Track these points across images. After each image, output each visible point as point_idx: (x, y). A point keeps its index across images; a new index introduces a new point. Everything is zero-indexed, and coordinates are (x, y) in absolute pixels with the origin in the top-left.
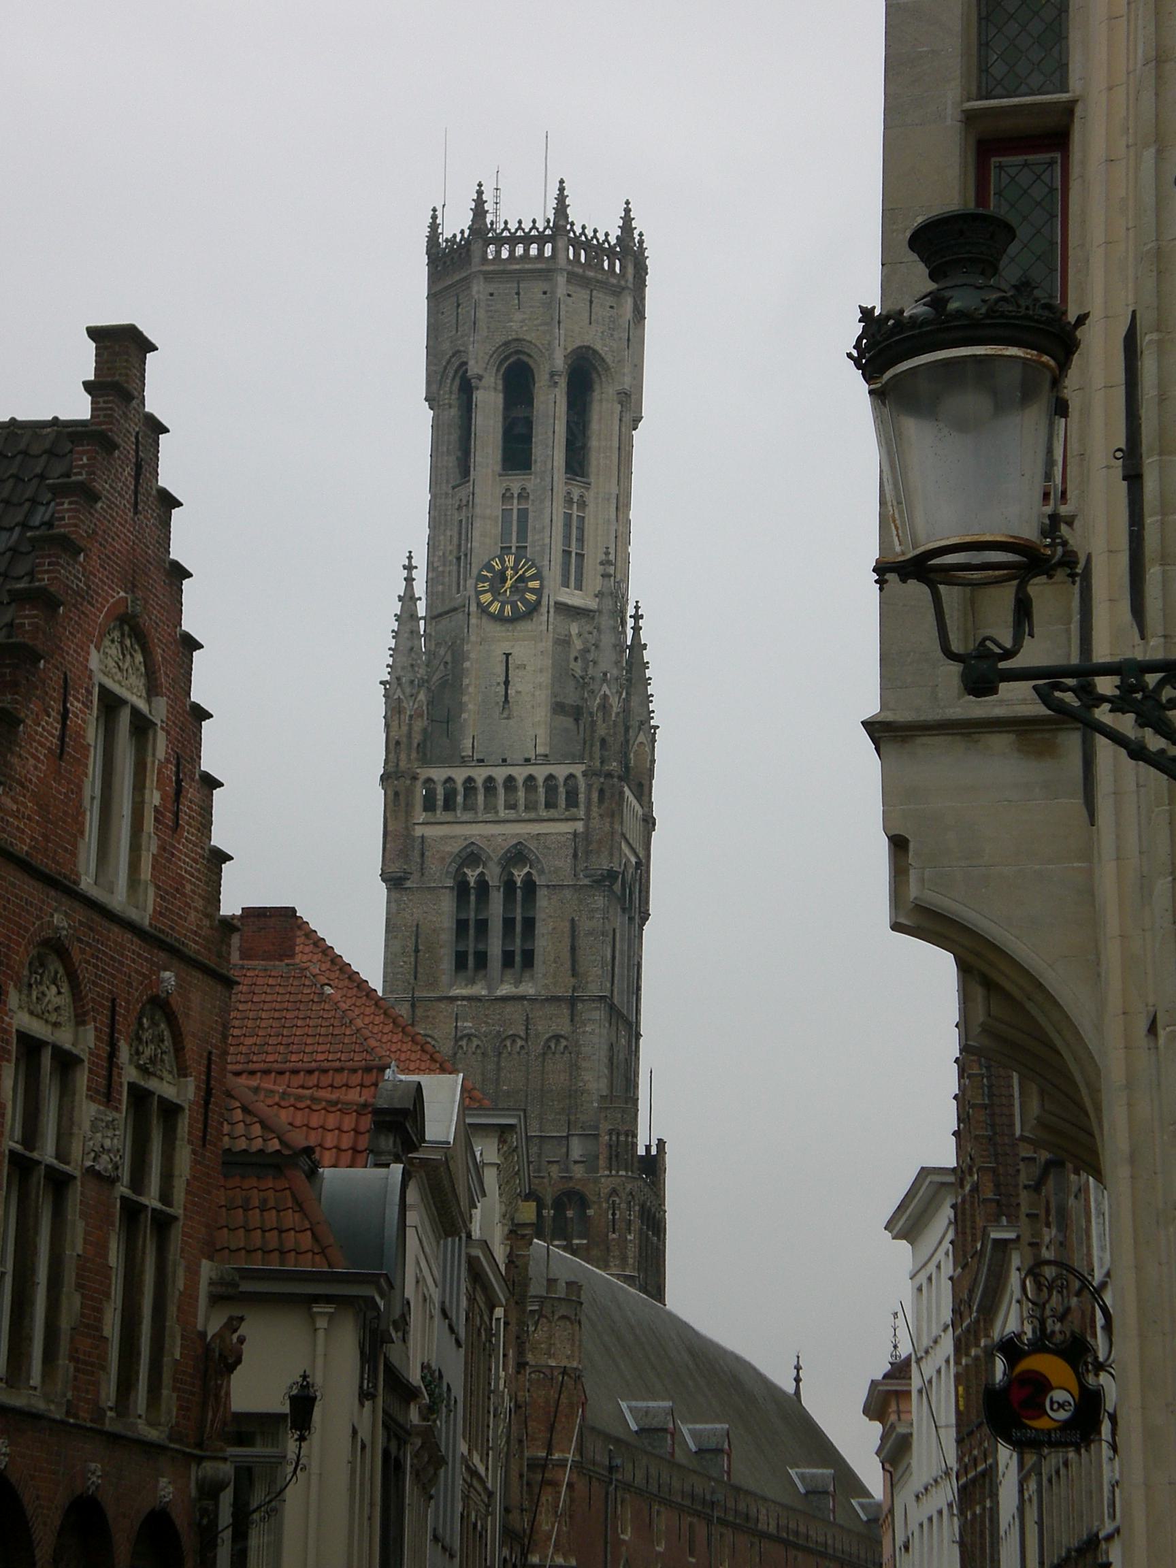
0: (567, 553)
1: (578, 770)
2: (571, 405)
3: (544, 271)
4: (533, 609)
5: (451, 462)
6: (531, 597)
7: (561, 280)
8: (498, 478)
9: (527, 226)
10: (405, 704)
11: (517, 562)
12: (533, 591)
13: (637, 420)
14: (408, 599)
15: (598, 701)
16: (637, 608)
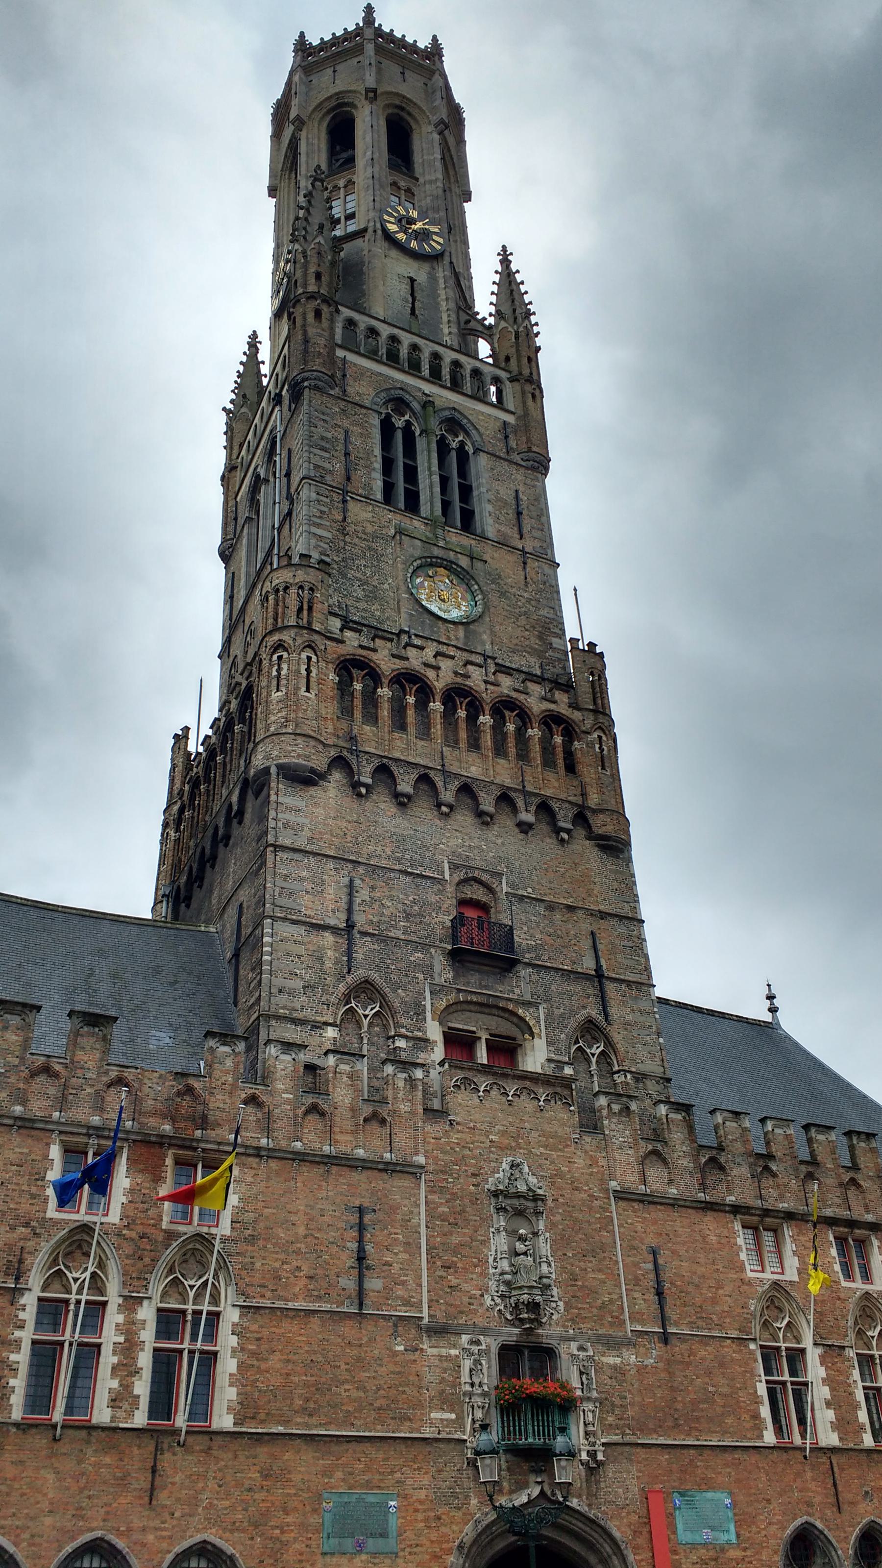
1: (503, 375)
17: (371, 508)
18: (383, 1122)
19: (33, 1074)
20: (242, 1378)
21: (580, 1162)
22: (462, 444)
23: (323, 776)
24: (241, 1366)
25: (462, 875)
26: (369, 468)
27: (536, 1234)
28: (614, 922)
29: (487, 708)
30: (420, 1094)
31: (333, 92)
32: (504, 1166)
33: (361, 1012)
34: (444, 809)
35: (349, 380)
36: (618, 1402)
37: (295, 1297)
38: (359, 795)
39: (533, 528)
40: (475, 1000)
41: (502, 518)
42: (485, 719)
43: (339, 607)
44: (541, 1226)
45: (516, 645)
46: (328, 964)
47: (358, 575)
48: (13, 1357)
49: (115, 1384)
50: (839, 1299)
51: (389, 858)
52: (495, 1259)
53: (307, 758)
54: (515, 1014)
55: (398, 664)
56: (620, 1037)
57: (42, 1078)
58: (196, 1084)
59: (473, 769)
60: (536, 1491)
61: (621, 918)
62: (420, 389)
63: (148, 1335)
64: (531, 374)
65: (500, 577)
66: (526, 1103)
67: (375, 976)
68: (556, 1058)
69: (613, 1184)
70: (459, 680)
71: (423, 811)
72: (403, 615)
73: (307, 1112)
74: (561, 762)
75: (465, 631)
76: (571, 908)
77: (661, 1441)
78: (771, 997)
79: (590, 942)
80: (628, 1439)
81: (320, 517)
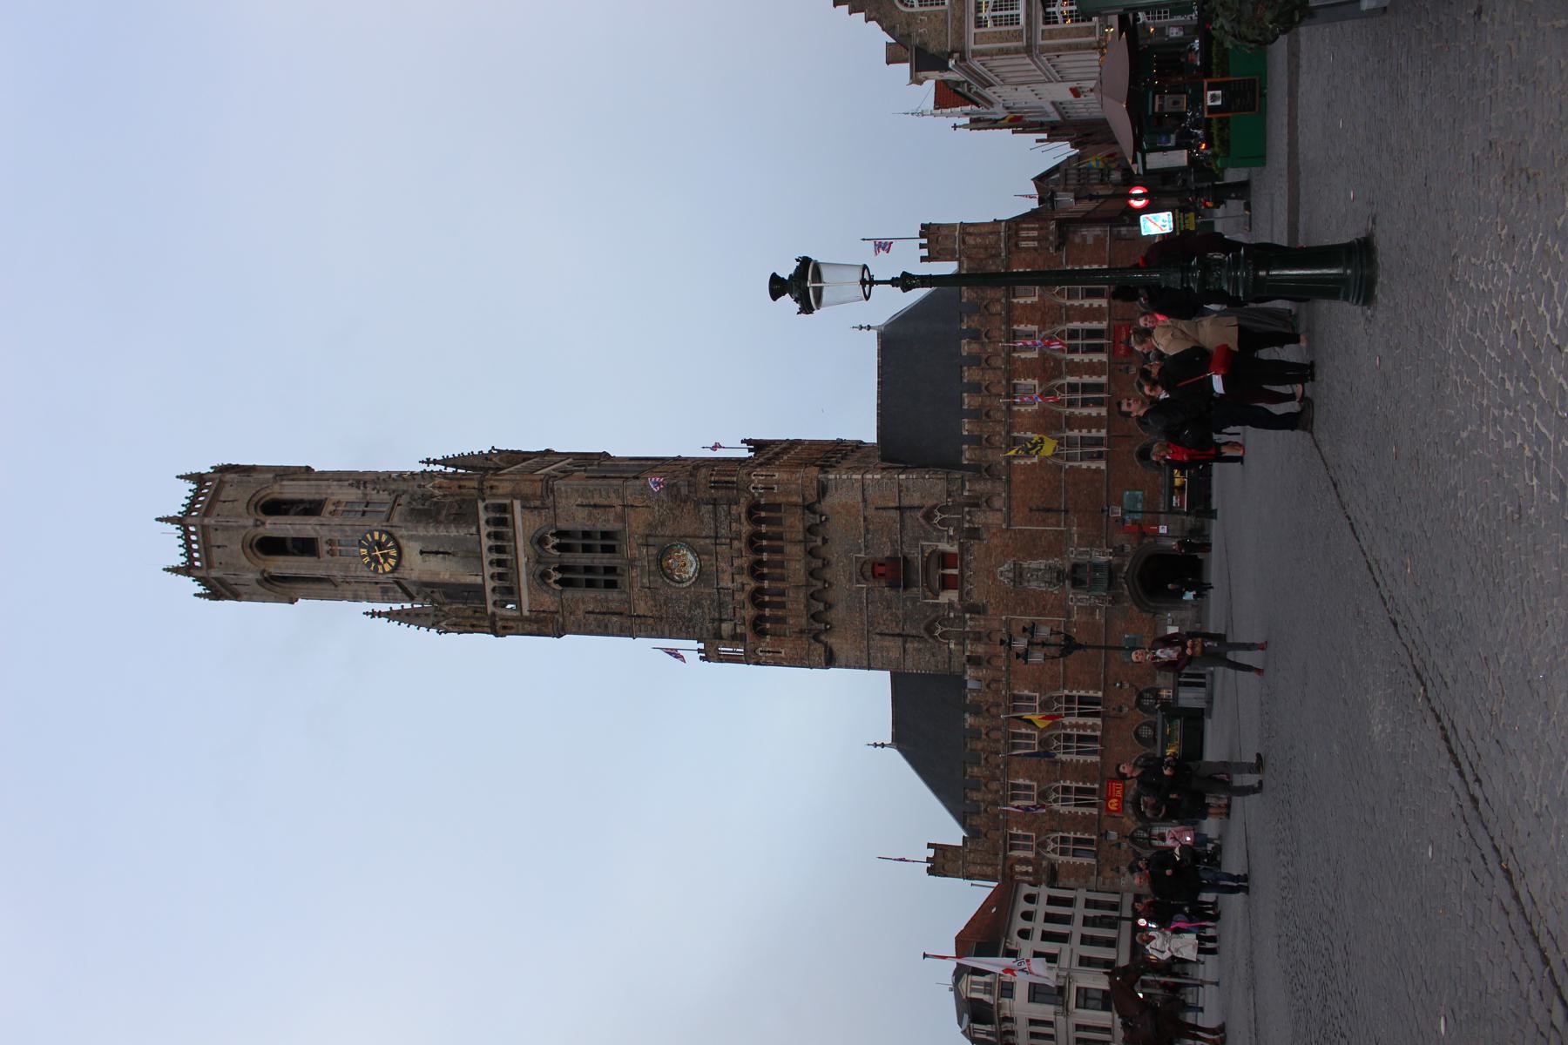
0: (364, 513)
1: (481, 505)
2: (286, 513)
3: (204, 531)
4: (390, 535)
5: (316, 586)
6: (384, 538)
7: (206, 521)
8: (321, 559)
9: (181, 542)
10: (449, 621)
11: (364, 547)
12: (380, 537)
13: (308, 468)
14: (391, 615)
15: (436, 491)
16: (423, 462)
17: (637, 602)
18: (990, 633)
19: (988, 762)
20: (1087, 689)
21: (995, 541)
22: (552, 535)
23: (826, 645)
24: (1083, 689)
25: (861, 578)
26: (606, 600)
27: (1029, 568)
28: (867, 496)
29: (758, 557)
30: (977, 616)
31: (257, 586)
32: (1002, 578)
33: (939, 631)
34: (827, 586)
35: (545, 608)
36: (1091, 539)
37: (1059, 669)
38: (831, 627)
39: (601, 496)
40: (924, 577)
41: (603, 518)
42: (765, 556)
43: (713, 623)
44: (1025, 565)
45: (696, 519)
46: (921, 646)
47: (687, 611)
48: (1081, 761)
49: (1089, 731)
50: (1044, 412)
51: (861, 615)
52: (1040, 587)
53: (820, 656)
54: (927, 557)
55: (747, 605)
56: (930, 501)
57: (989, 759)
58: (985, 708)
59: (797, 567)
60: (1123, 580)
61: (863, 490)
62: (527, 564)
63: (1074, 720)
64: (474, 488)
65: (649, 524)
66: (973, 565)
67: (922, 626)
68: (945, 540)
69: (1004, 526)
70: (746, 572)
71: (830, 596)
72: (707, 591)
73: (990, 664)
74: (779, 515)
75: (703, 554)
76: (865, 519)
77: (1105, 520)
78: (861, 328)
79: (881, 511)
80: (1105, 535)
81: (657, 630)
